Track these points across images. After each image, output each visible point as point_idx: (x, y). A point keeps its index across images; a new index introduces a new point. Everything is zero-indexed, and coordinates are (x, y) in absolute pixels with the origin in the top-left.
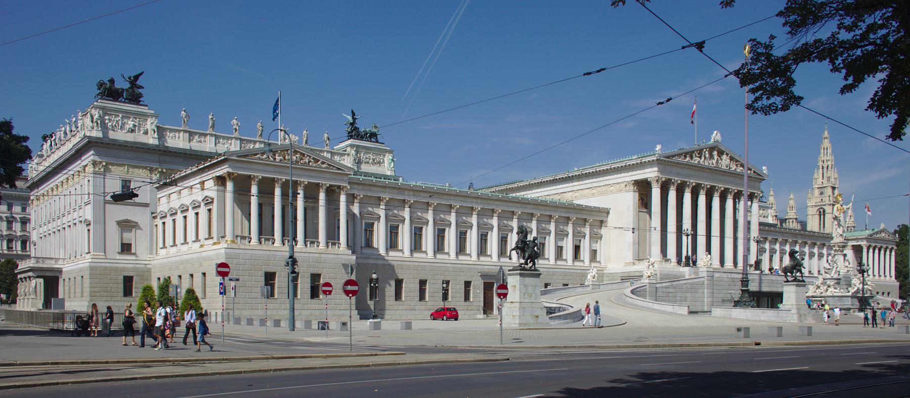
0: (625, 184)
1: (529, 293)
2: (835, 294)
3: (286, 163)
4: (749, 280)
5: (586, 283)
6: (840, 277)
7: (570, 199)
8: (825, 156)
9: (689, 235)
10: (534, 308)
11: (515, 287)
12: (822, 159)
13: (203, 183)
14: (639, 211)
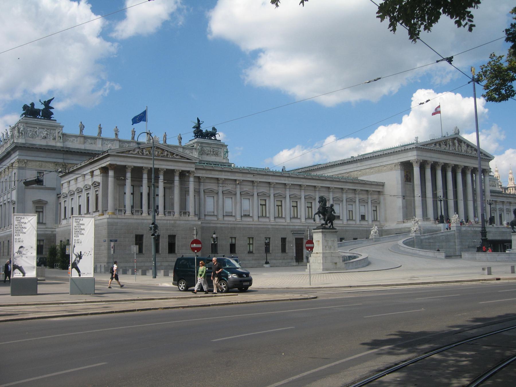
0: (394, 165)
1: (329, 246)
3: (150, 156)
4: (487, 232)
7: (356, 176)
9: (442, 201)
10: (334, 256)
11: (319, 241)
13: (92, 172)
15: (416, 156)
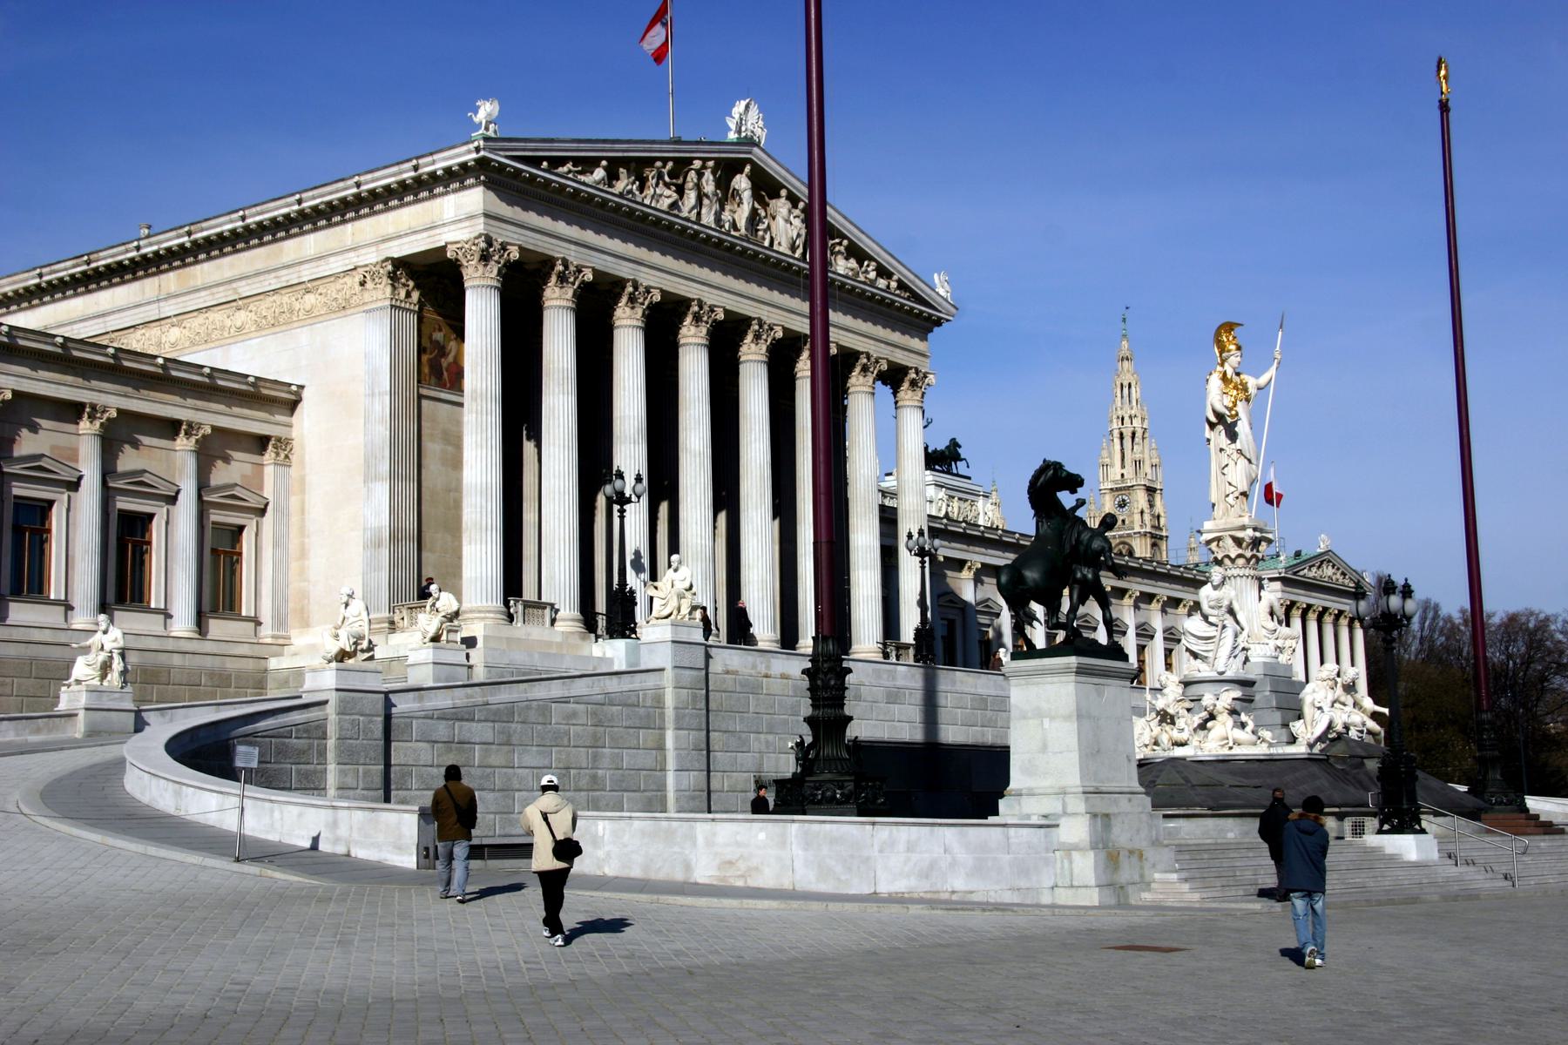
0: (358, 278)
2: (1237, 751)
5: (63, 706)
6: (1251, 676)
8: (1127, 406)
9: (629, 501)
12: (1120, 413)
14: (420, 397)
15: (482, 220)
